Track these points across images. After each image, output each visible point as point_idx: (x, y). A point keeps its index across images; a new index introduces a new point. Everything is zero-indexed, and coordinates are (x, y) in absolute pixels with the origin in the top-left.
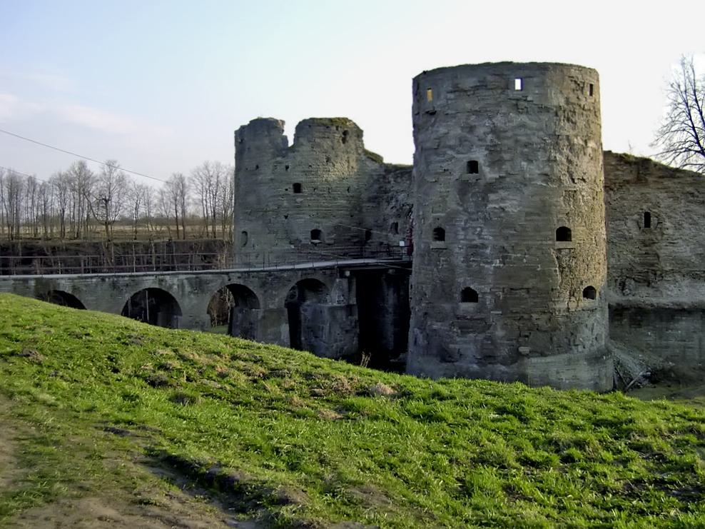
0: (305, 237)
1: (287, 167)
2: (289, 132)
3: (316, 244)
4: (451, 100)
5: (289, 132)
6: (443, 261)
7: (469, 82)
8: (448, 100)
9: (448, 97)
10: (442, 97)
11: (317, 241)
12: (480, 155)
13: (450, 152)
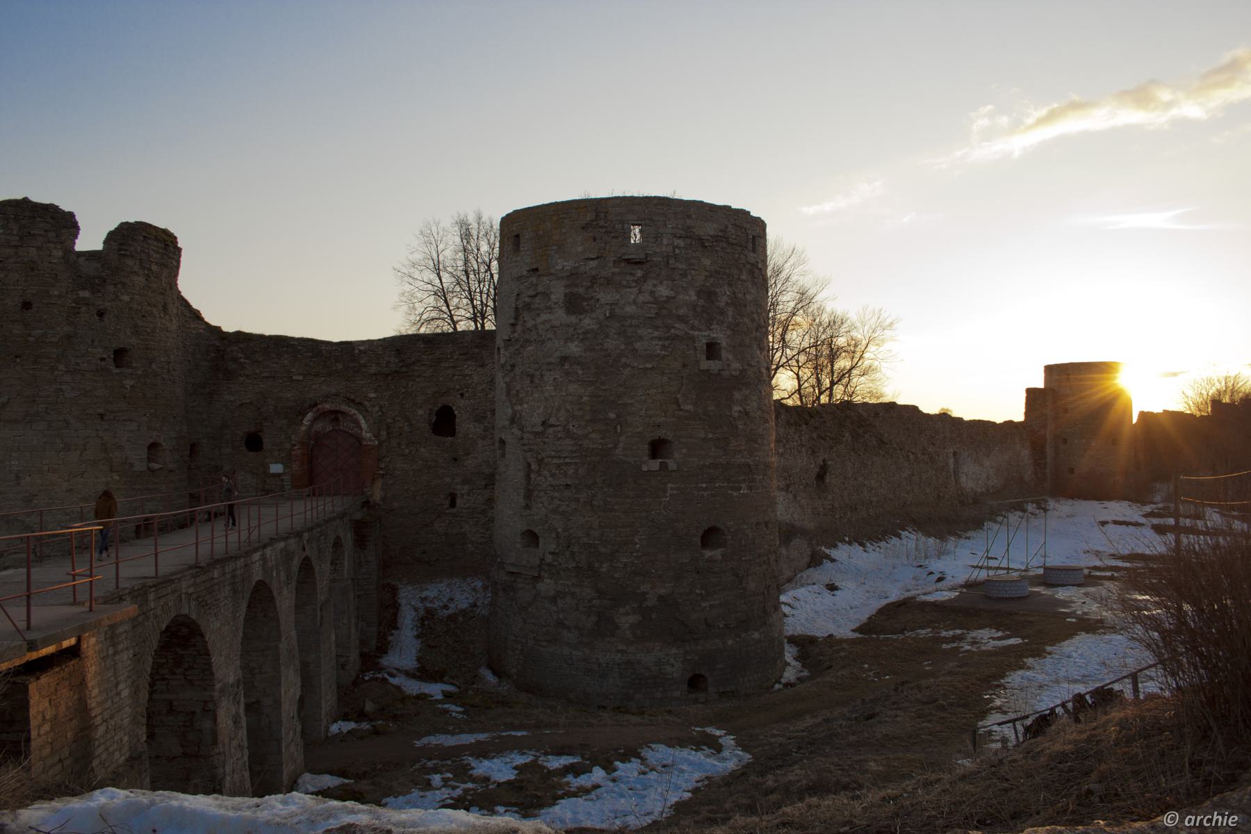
3: (152, 471)
4: (679, 248)
6: (671, 489)
7: (709, 229)
8: (675, 247)
9: (676, 244)
11: (157, 466)
12: (720, 335)
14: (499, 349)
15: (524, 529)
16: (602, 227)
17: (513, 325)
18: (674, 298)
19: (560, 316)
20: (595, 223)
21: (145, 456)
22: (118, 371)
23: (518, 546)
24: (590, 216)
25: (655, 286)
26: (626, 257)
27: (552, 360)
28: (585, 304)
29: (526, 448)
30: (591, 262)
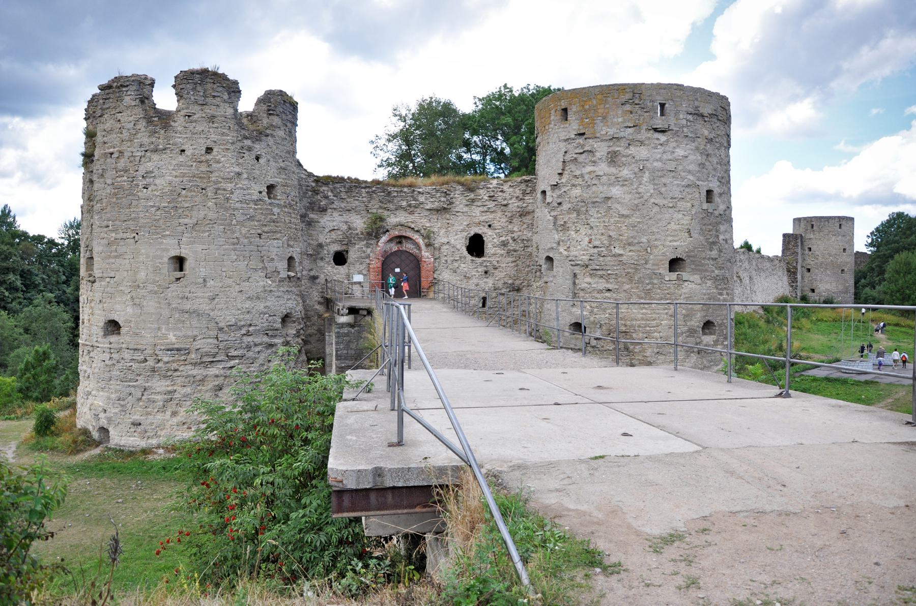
0: (282, 265)
1: (257, 158)
2: (247, 104)
4: (690, 121)
5: (247, 104)
10: (681, 116)
13: (691, 178)
14: (544, 192)
15: (573, 321)
16: (636, 104)
17: (560, 174)
18: (687, 157)
19: (603, 168)
20: (631, 101)
21: (286, 266)
22: (269, 201)
23: (567, 334)
24: (628, 96)
25: (674, 148)
26: (655, 127)
27: (597, 200)
28: (624, 159)
29: (572, 263)
30: (629, 129)
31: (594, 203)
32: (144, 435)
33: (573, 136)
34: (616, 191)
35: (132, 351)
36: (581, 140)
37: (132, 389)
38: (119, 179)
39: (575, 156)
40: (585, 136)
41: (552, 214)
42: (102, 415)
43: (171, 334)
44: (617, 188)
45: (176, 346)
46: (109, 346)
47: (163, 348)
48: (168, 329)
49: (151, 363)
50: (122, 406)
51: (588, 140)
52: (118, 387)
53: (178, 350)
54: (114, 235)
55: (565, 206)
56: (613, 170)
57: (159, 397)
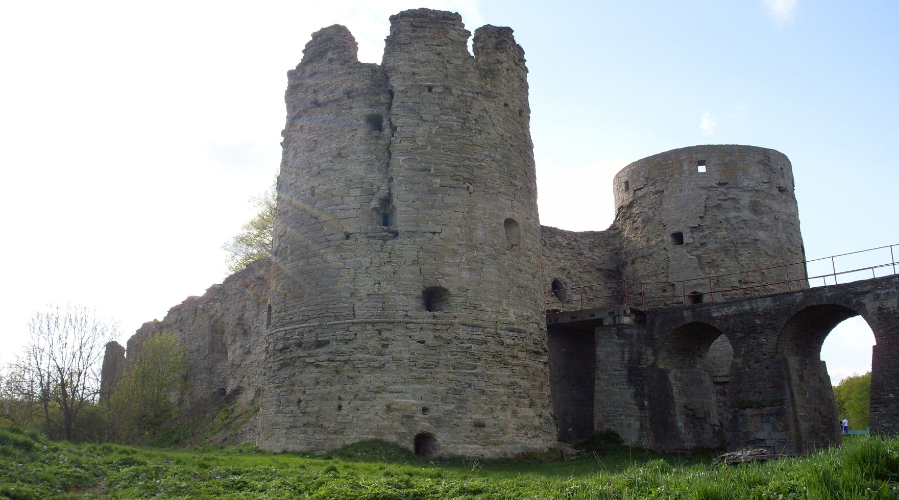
17: (701, 218)
19: (747, 214)
24: (761, 157)
28: (763, 208)
31: (744, 243)
32: (486, 441)
33: (715, 185)
34: (761, 235)
35: (470, 328)
36: (723, 189)
37: (473, 378)
38: (445, 118)
39: (719, 202)
40: (728, 186)
41: (694, 253)
42: (419, 416)
43: (512, 311)
44: (762, 232)
45: (516, 327)
46: (434, 321)
47: (505, 327)
48: (508, 304)
49: (493, 346)
50: (461, 400)
51: (730, 189)
52: (451, 376)
53: (519, 331)
54: (438, 181)
55: (712, 246)
56: (754, 217)
57: (502, 390)
